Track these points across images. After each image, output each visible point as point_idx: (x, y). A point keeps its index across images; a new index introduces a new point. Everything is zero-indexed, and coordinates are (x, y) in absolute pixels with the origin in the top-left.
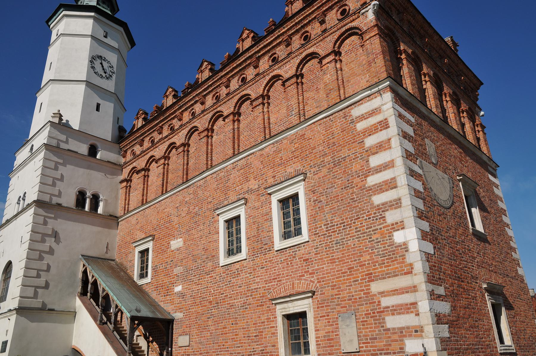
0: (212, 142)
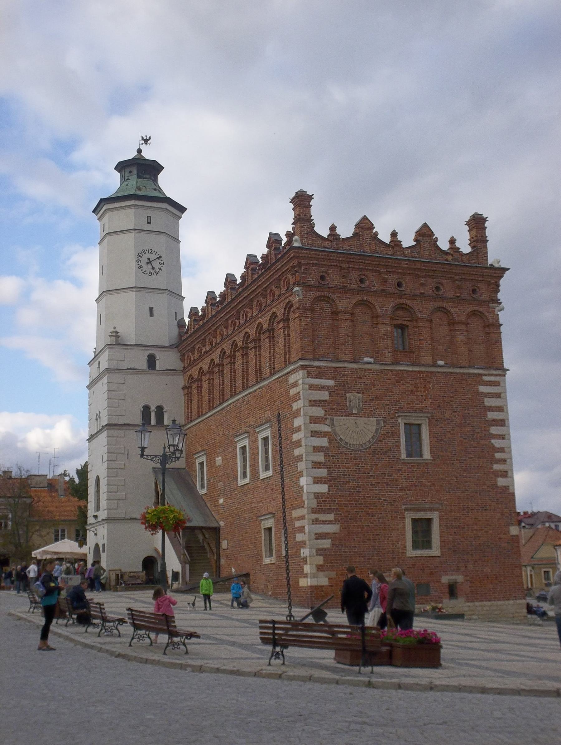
0: (234, 368)
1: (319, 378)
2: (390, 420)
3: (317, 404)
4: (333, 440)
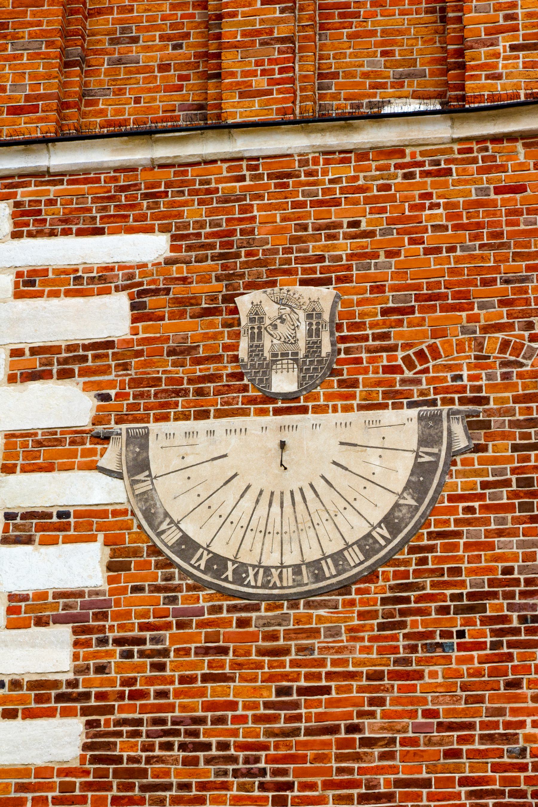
1: (81, 233)
2: (510, 412)
3: (55, 369)
4: (136, 552)
